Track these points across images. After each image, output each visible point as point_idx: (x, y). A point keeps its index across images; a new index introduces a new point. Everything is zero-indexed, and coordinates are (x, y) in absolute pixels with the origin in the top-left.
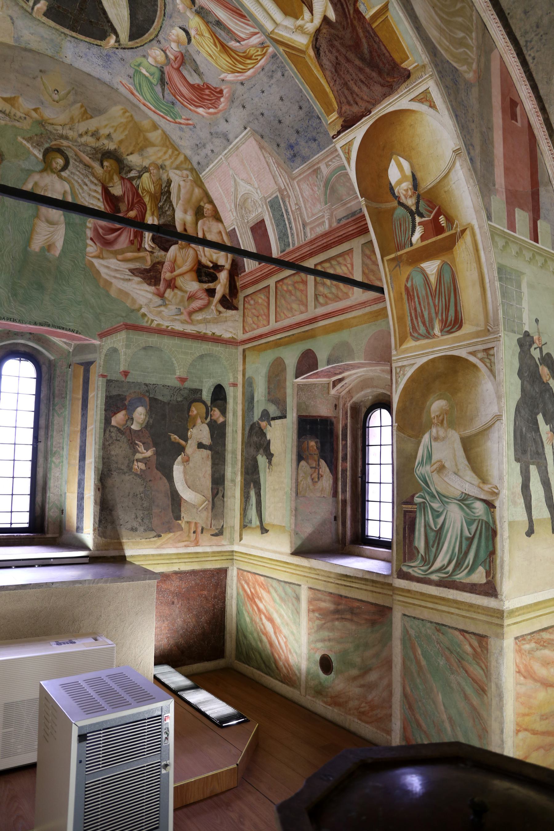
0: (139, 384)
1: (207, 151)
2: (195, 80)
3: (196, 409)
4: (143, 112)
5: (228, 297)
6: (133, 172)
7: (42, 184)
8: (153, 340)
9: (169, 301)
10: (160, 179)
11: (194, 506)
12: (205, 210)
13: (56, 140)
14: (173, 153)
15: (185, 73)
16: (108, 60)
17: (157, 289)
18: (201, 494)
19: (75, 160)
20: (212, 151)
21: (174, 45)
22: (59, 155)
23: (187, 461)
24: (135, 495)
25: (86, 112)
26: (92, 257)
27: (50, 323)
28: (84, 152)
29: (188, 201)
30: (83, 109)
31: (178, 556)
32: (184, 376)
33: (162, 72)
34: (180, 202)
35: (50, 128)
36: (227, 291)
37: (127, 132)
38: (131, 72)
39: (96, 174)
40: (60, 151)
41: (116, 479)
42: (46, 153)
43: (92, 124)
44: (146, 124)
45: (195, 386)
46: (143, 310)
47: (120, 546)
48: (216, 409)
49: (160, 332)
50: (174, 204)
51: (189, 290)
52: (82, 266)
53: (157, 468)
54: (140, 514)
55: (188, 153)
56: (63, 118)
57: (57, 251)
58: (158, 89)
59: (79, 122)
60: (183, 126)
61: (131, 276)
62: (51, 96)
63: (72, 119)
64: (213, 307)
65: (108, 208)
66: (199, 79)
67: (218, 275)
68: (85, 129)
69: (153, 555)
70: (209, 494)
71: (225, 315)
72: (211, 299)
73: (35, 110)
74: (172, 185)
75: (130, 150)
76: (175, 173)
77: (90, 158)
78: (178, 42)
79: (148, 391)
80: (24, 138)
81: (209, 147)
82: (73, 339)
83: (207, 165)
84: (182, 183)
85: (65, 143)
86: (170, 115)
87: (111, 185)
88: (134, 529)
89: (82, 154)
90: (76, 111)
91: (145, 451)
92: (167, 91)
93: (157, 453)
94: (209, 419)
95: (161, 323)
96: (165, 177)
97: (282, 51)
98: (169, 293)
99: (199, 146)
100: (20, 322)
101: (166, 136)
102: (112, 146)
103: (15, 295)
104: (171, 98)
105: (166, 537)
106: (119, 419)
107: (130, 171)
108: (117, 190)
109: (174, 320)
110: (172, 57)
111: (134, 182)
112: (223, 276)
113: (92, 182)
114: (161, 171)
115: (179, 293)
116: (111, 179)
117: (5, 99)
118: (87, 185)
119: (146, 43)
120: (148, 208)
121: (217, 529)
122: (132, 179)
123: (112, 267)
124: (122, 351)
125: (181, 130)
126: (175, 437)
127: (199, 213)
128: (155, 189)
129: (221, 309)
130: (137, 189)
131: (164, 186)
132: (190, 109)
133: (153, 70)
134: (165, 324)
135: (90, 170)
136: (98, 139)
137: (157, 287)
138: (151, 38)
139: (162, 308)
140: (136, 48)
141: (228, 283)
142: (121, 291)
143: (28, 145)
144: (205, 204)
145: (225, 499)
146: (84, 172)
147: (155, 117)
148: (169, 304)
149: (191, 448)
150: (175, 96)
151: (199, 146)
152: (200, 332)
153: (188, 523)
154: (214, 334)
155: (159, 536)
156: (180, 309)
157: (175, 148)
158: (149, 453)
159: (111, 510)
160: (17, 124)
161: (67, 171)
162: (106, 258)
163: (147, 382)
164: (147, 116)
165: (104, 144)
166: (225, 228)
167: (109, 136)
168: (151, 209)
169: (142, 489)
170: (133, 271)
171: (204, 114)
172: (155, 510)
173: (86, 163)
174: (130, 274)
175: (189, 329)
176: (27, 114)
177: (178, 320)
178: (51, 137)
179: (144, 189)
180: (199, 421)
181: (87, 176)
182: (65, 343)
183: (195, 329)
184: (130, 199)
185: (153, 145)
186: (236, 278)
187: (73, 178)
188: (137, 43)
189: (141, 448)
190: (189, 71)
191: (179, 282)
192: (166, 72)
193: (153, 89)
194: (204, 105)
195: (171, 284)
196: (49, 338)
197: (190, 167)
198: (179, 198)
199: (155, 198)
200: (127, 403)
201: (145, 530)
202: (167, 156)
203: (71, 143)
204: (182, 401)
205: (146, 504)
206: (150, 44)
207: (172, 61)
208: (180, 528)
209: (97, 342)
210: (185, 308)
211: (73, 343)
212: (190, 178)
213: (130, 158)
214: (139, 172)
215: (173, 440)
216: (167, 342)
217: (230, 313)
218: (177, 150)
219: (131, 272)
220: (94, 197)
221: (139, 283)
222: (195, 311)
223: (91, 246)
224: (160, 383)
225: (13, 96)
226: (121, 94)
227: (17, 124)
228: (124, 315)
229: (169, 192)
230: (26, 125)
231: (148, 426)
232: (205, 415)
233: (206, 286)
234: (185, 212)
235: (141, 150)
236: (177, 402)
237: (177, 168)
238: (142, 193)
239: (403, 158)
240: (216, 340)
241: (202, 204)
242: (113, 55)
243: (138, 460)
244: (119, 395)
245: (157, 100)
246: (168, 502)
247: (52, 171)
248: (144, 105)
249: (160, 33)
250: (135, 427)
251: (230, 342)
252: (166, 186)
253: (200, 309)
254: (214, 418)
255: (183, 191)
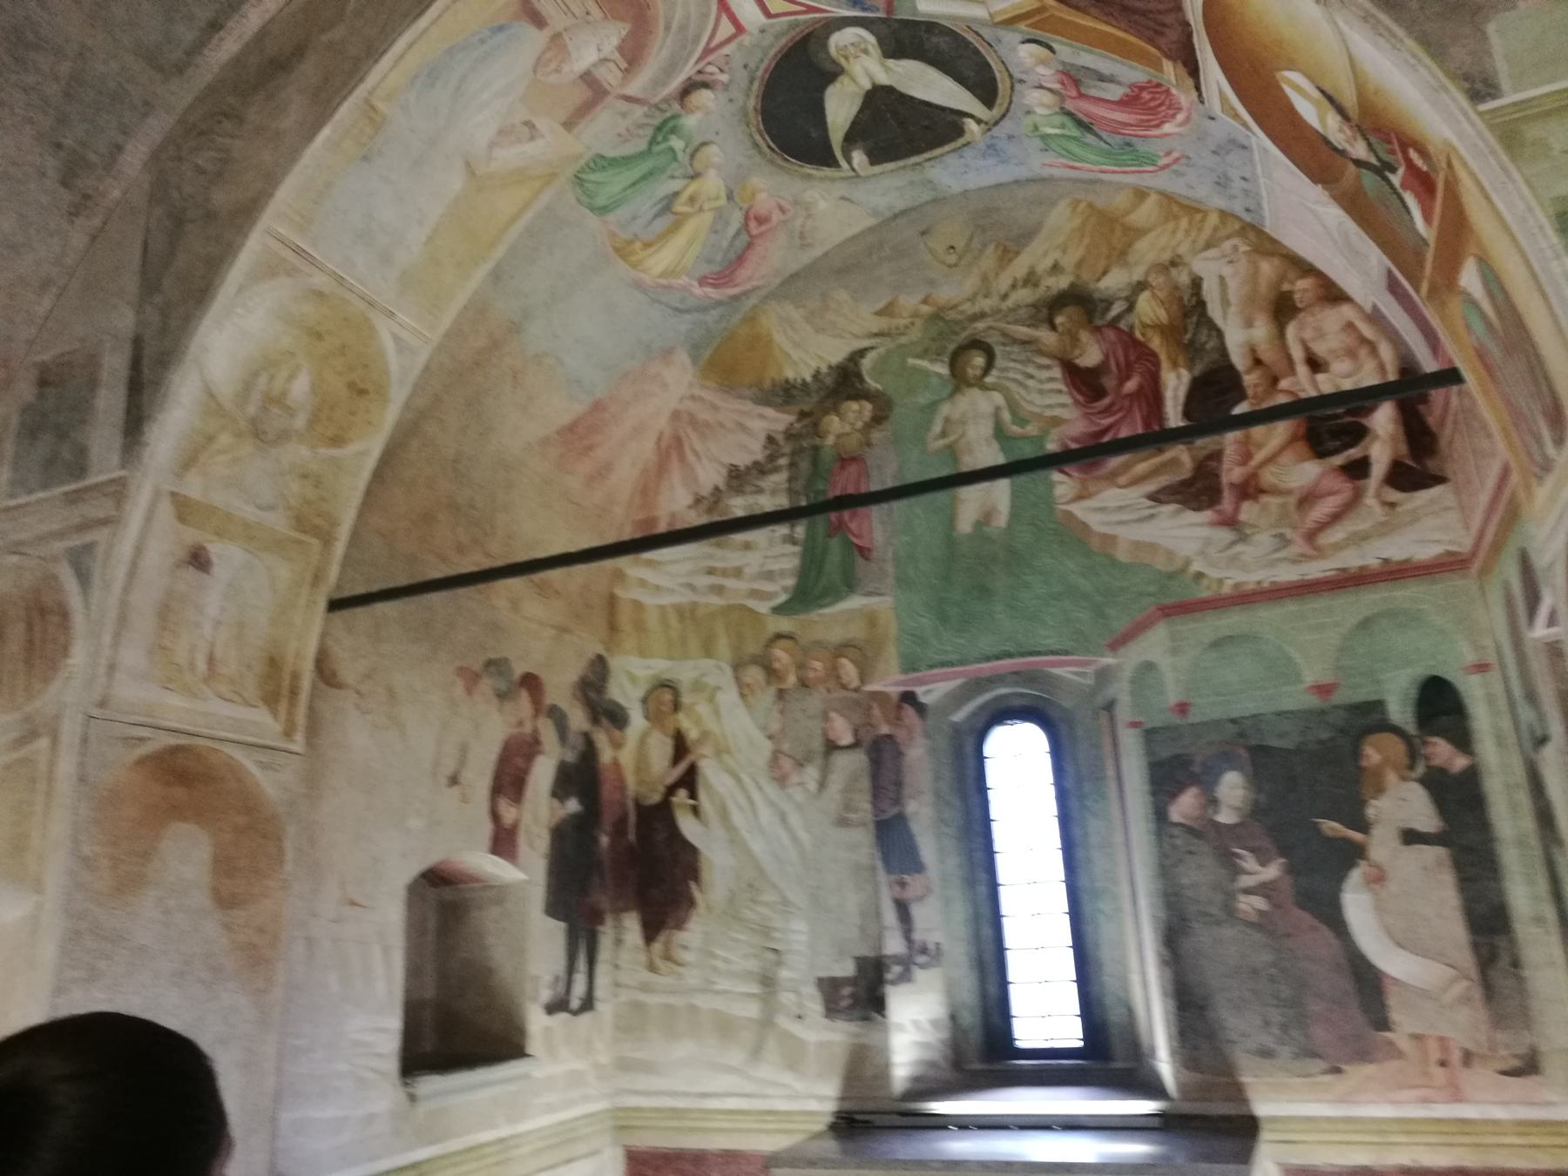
0: (1216, 724)
1: (1238, 184)
2: (1115, 92)
3: (1379, 751)
4: (1110, 183)
5: (1410, 462)
6: (1115, 306)
7: (956, 415)
8: (1233, 621)
9: (1254, 526)
10: (1176, 288)
11: (1424, 993)
12: (1297, 296)
13: (964, 329)
14: (1190, 222)
15: (1093, 92)
16: (995, 150)
17: (1217, 511)
18: (1439, 961)
19: (1004, 344)
20: (1244, 179)
21: (1041, 70)
22: (974, 352)
23: (1378, 878)
24: (1255, 972)
25: (1006, 250)
26: (1069, 502)
27: (1012, 650)
28: (1016, 322)
29: (1251, 300)
30: (1001, 248)
31: (1407, 1126)
32: (1327, 679)
33: (1069, 114)
34: (1233, 309)
35: (952, 315)
36: (1403, 449)
37: (1086, 241)
38: (1038, 143)
39: (1044, 348)
40: (977, 344)
41: (1202, 937)
42: (956, 361)
43: (1019, 268)
44: (1121, 201)
45: (1363, 695)
46: (1196, 567)
47: (1237, 1093)
48: (1435, 739)
49: (1244, 598)
50: (1219, 322)
51: (1293, 485)
52: (1052, 526)
53: (1302, 907)
54: (1275, 1015)
55: (1219, 202)
56: (971, 284)
57: (1002, 520)
58: (1090, 139)
59: (997, 274)
60: (1175, 167)
61: (1150, 507)
62: (943, 263)
63: (985, 279)
64: (1370, 500)
65: (1080, 398)
66: (1118, 86)
67: (1365, 421)
68: (1009, 282)
69: (1329, 1119)
70: (1467, 960)
71: (1409, 506)
72: (1362, 482)
73: (925, 302)
74: (1205, 286)
75: (1100, 269)
76: (1207, 259)
77: (1029, 326)
78: (1043, 62)
79: (1242, 735)
80: (918, 357)
81: (1234, 174)
82: (1086, 664)
83: (1259, 205)
84: (1227, 271)
85: (980, 325)
86: (1145, 163)
87: (1077, 352)
88: (1266, 1053)
89: (1013, 327)
90: (988, 261)
91: (1259, 868)
92: (1104, 135)
93: (1291, 870)
94: (1420, 770)
95: (1244, 579)
96: (1183, 278)
97: (1026, 28)
98: (1248, 512)
99: (1222, 183)
100: (962, 663)
101: (1167, 198)
102: (1062, 283)
103: (943, 618)
104: (1117, 139)
105: (1358, 1073)
106: (1185, 806)
107: (1108, 309)
108: (1090, 355)
109: (1273, 564)
110: (1057, 86)
111: (1123, 325)
112: (1383, 419)
113: (1041, 367)
114: (1174, 272)
115: (1272, 501)
116: (1075, 340)
117: (880, 313)
118: (1032, 377)
119: (1011, 96)
120: (1163, 357)
121: (1516, 1056)
122: (1119, 317)
123: (1112, 504)
124: (1165, 663)
125: (1179, 174)
126: (1331, 827)
127: (1283, 309)
128: (1168, 313)
129: (1394, 495)
130: (1131, 335)
131: (1186, 299)
132: (1156, 137)
133: (1059, 119)
134: (1253, 578)
135: (1034, 348)
136: (1036, 285)
137: (1218, 508)
138: (1008, 84)
139: (1239, 548)
140: (1008, 110)
141: (1401, 431)
142: (1138, 545)
143: (924, 364)
144: (1292, 283)
145: (1526, 973)
146: (1023, 357)
147: (1131, 179)
148: (1253, 534)
149: (1382, 845)
150: (1120, 133)
151: (1222, 183)
152: (1343, 570)
153: (1417, 1037)
154: (1386, 561)
155: (1337, 1071)
156: (1281, 536)
157: (1193, 210)
158: (1272, 872)
159: (1202, 1008)
160: (903, 340)
161: (994, 372)
162: (1097, 493)
163: (1235, 714)
164: (1120, 187)
165: (1047, 287)
166: (1360, 309)
167: (1056, 268)
168: (1169, 358)
169: (1267, 957)
170: (1156, 498)
171: (1178, 130)
172: (1315, 1007)
173: (1024, 338)
174: (1153, 503)
175: (1316, 570)
176: (915, 315)
177: (1285, 559)
178: (957, 329)
179: (1145, 326)
180: (1391, 778)
181: (1029, 361)
182: (1076, 673)
183: (1336, 567)
184: (1122, 359)
185: (1140, 232)
186: (1421, 408)
187: (1008, 379)
188: (1000, 105)
189: (1249, 862)
190: (1094, 87)
191: (1268, 477)
192: (1073, 111)
193: (1085, 144)
194: (1164, 117)
195: (1250, 490)
196: (1050, 673)
197: (1237, 226)
198: (1225, 302)
199: (1171, 332)
200: (1196, 769)
201: (1297, 1056)
202: (1180, 235)
203: (989, 319)
204: (1332, 739)
205: (1286, 992)
206: (1015, 93)
207: (1063, 92)
208: (1395, 1053)
209: (1108, 660)
210: (1294, 528)
211: (1090, 670)
212: (1244, 248)
213: (1103, 284)
214: (1127, 299)
215: (1329, 833)
216: (1265, 617)
217: (1423, 497)
218: (1198, 211)
219: (1154, 501)
220: (1052, 391)
221: (1177, 512)
222: (1323, 526)
223: (1062, 483)
224: (1265, 708)
225: (889, 299)
226: (1061, 179)
227: (903, 340)
228: (1152, 589)
229: (1201, 304)
230: (915, 334)
231: (1256, 812)
232: (1406, 761)
233: (1338, 460)
234: (1249, 324)
235: (1121, 256)
236: (1321, 742)
237: (1208, 246)
238: (1143, 335)
239: (1290, 70)
240: (1396, 572)
241: (1286, 287)
242: (995, 141)
243: (1248, 891)
244: (1177, 757)
245: (1108, 154)
246: (1346, 984)
247: (970, 385)
248: (1102, 172)
249: (1010, 69)
250: (1225, 817)
251: (1442, 565)
252: (1192, 295)
253: (1336, 518)
254: (1436, 762)
255: (1232, 284)
